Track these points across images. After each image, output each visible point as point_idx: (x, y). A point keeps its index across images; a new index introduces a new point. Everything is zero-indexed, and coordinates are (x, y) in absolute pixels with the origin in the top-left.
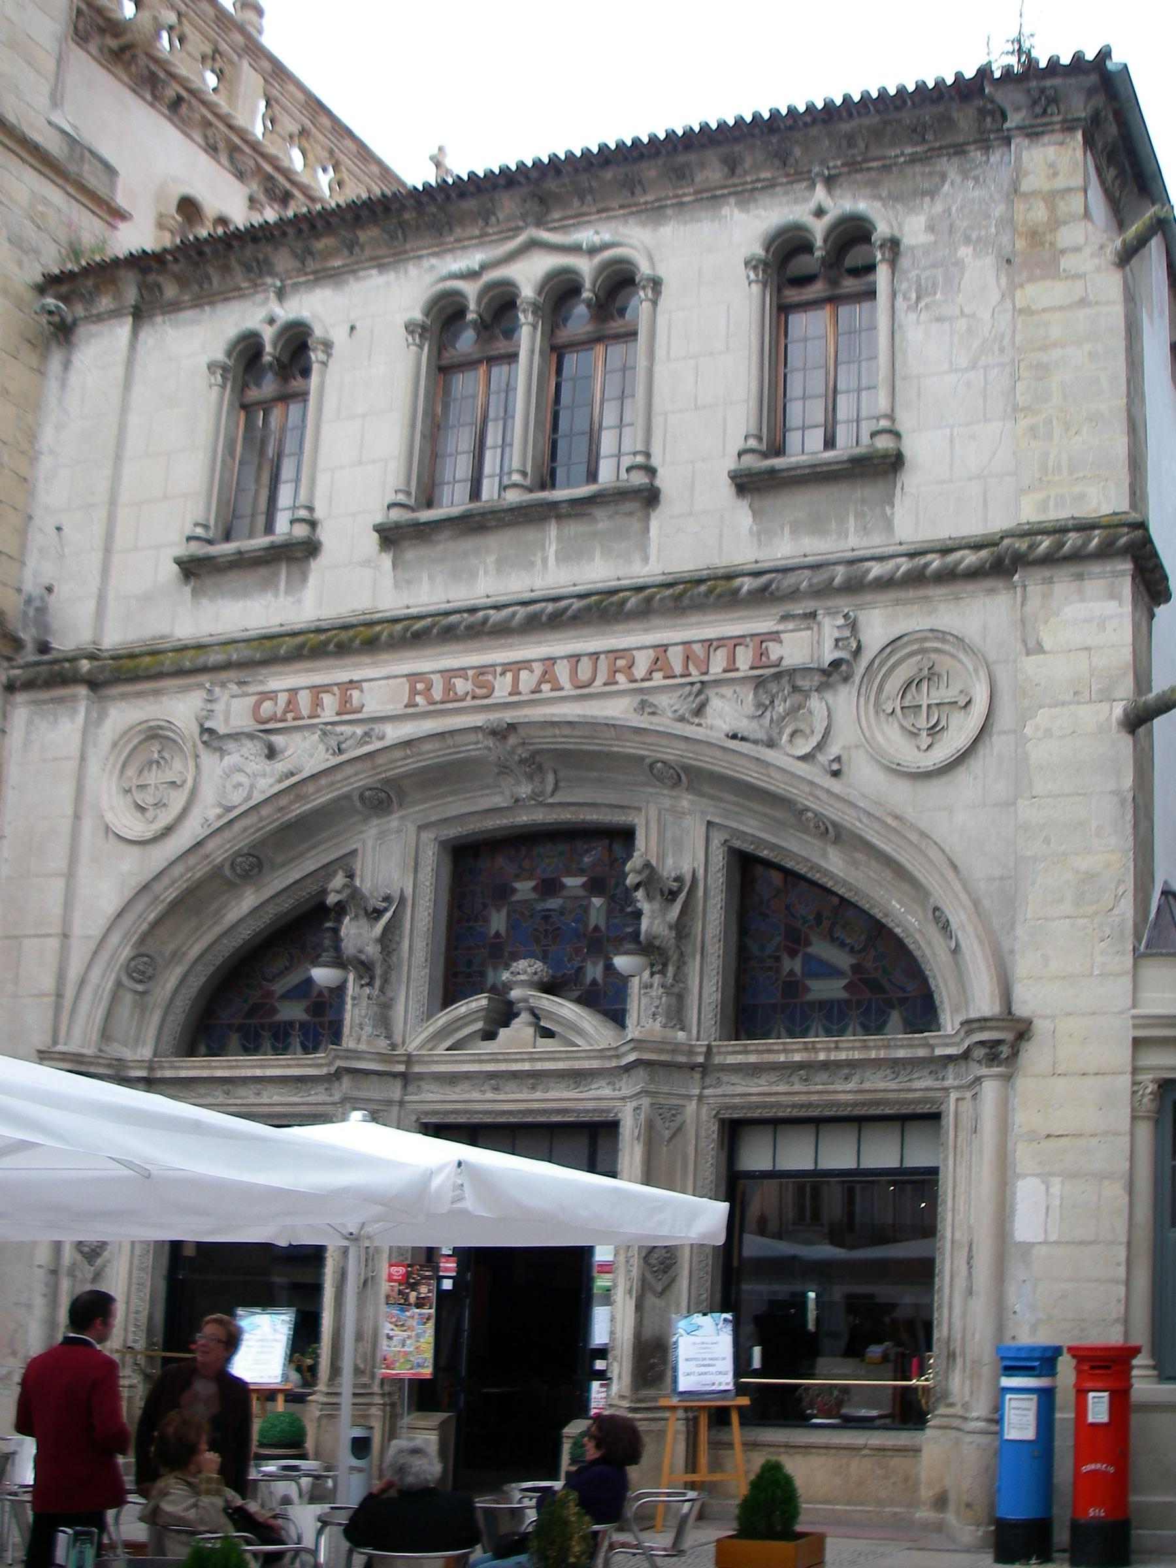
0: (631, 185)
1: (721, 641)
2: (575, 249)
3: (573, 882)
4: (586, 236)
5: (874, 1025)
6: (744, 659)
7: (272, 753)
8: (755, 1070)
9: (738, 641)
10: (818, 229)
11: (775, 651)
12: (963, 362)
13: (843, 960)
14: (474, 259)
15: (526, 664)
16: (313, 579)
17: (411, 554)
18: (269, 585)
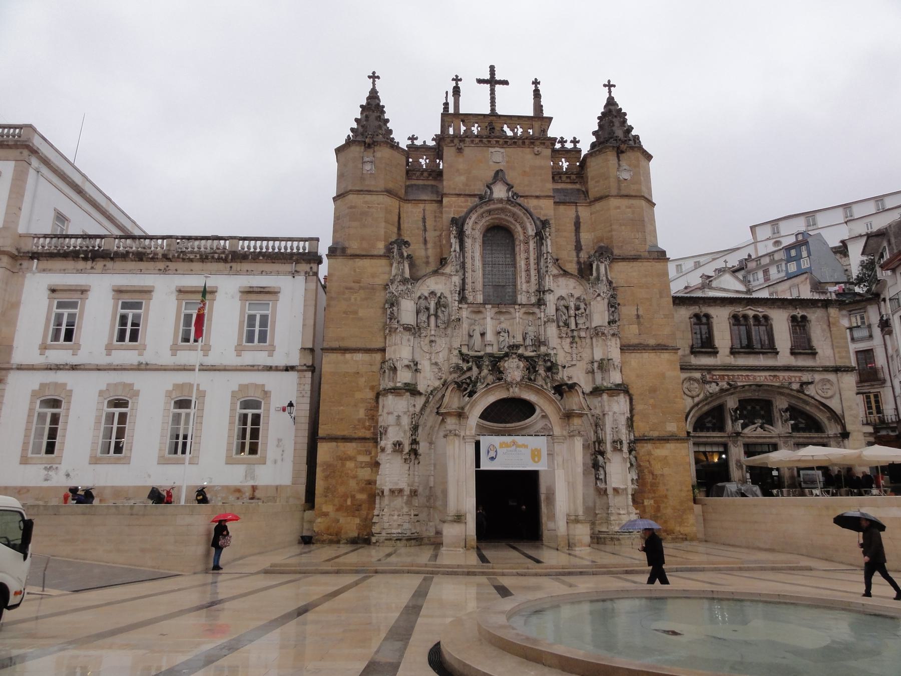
0: (765, 303)
1: (793, 376)
2: (758, 311)
3: (758, 408)
4: (760, 310)
5: (810, 431)
6: (797, 380)
7: (717, 385)
8: (800, 437)
9: (797, 376)
10: (799, 316)
11: (802, 379)
12: (823, 339)
13: (803, 421)
14: (741, 309)
15: (762, 376)
16: (718, 358)
17: (737, 356)
18: (710, 356)
